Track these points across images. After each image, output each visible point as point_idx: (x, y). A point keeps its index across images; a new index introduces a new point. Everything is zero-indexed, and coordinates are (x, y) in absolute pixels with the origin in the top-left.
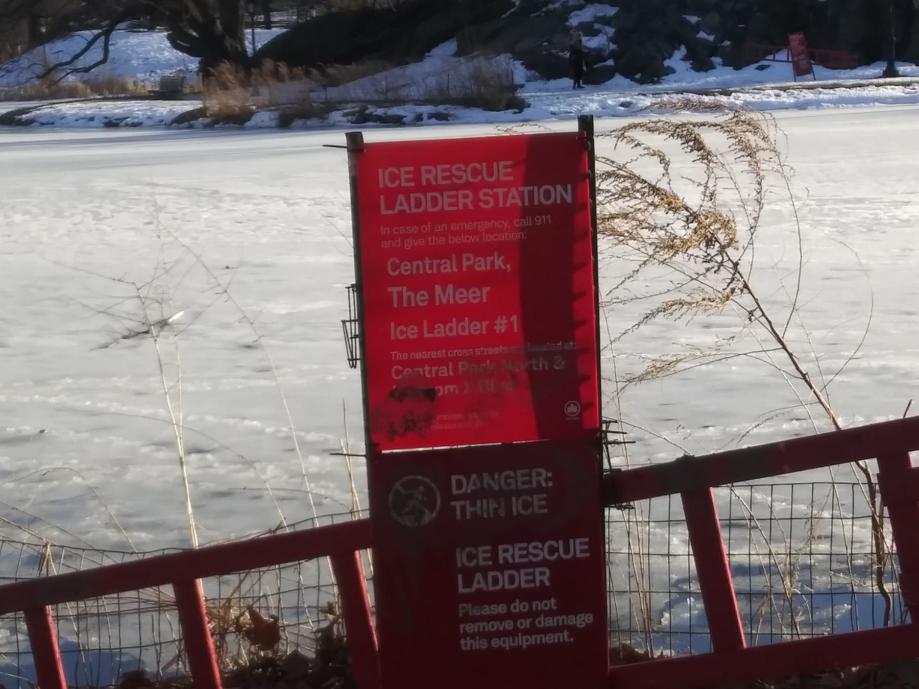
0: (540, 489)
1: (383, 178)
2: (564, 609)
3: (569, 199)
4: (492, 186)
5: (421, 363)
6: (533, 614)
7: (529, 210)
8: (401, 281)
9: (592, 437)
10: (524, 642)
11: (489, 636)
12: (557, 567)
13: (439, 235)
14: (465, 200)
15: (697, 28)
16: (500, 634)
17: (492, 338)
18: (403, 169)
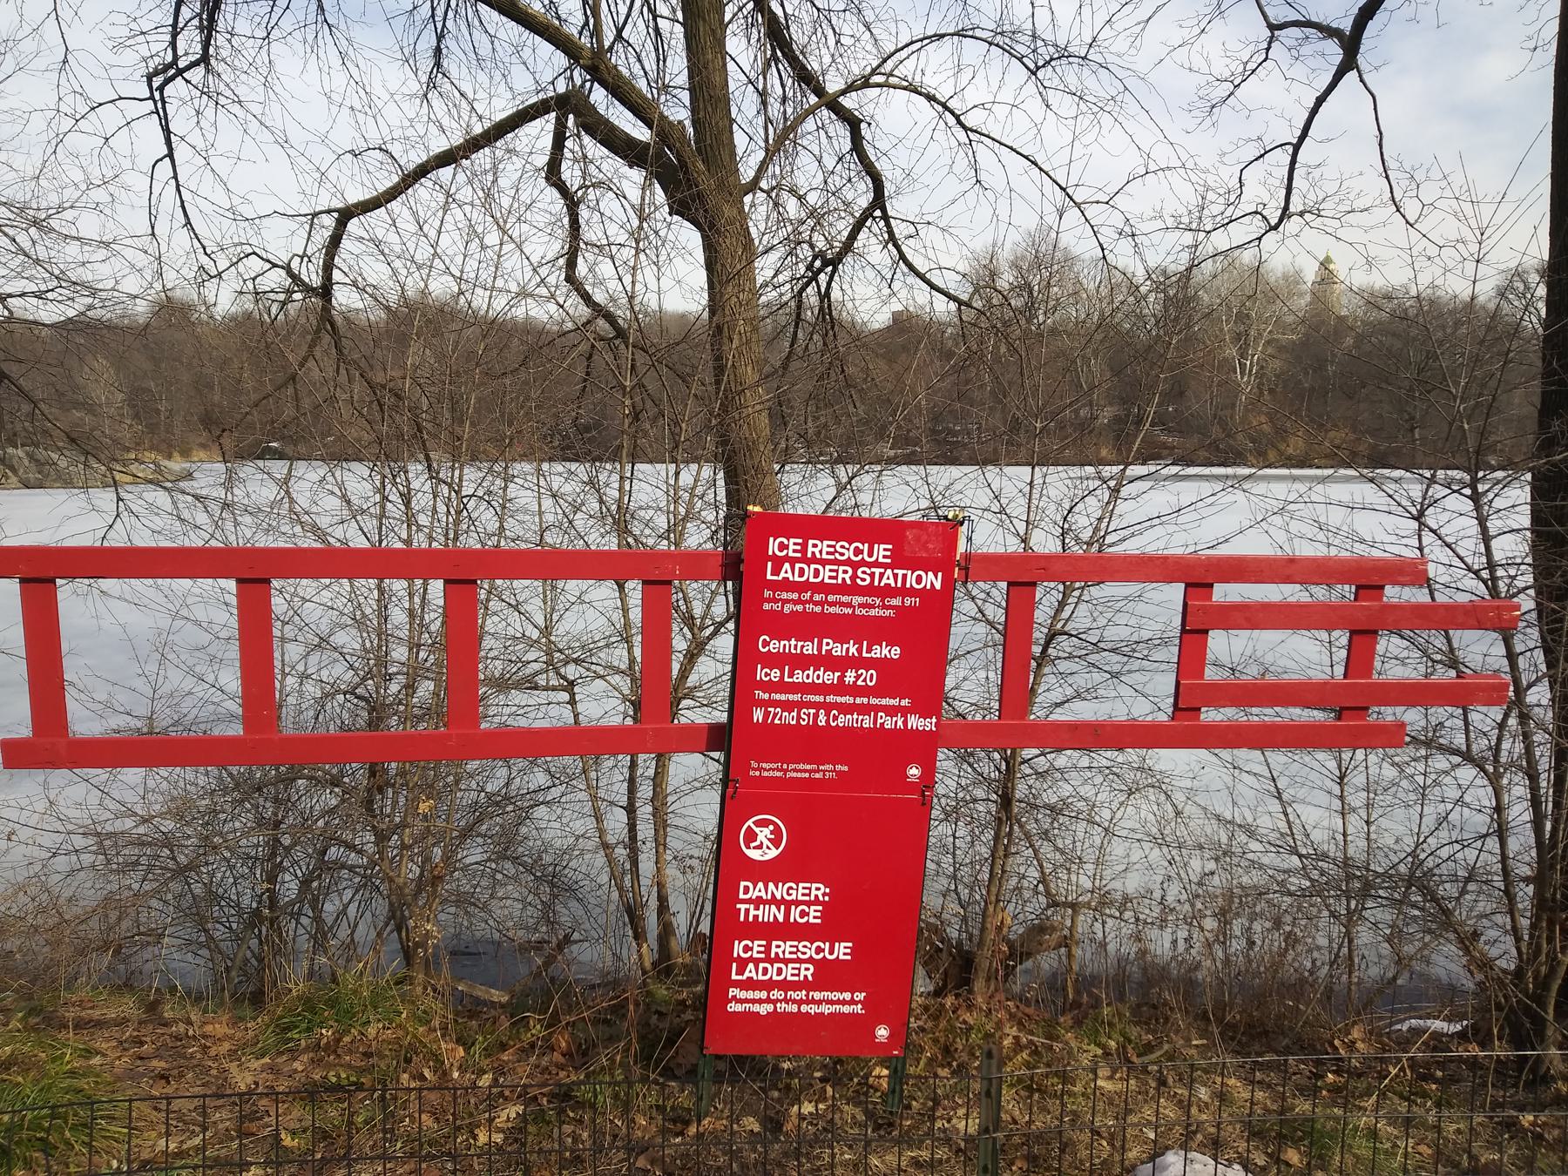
3: (938, 586)
4: (870, 565)
13: (816, 603)
14: (844, 574)
18: (792, 540)
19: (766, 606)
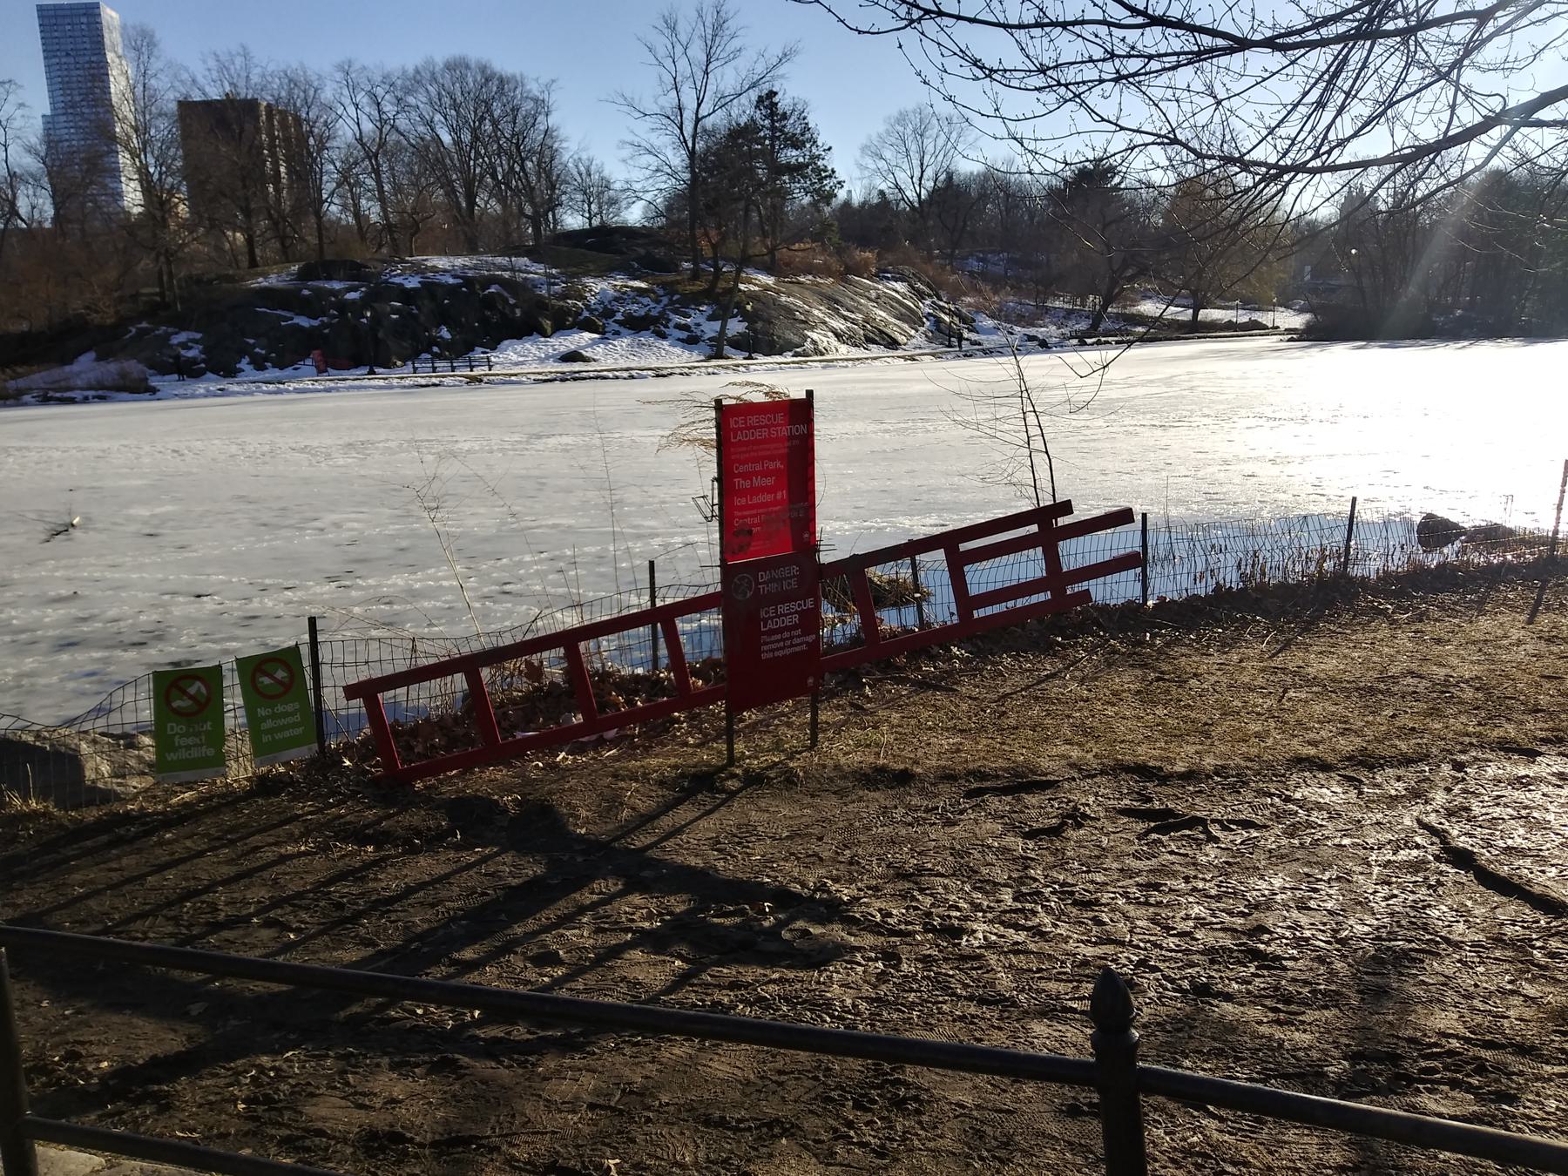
6: (791, 638)
7: (791, 438)
9: (813, 547)
10: (787, 652)
15: (254, 346)
17: (775, 503)
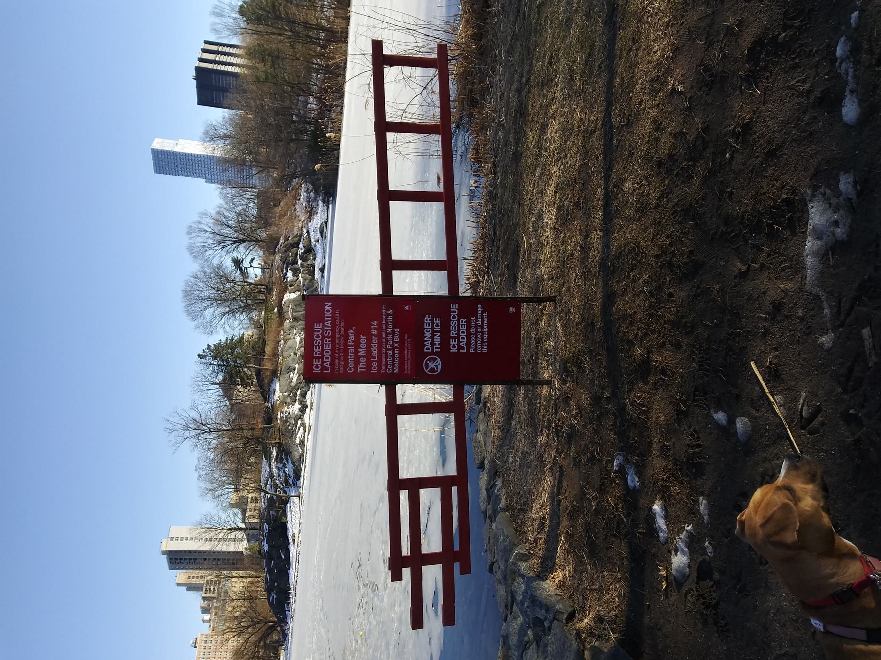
0: (432, 320)
1: (317, 370)
2: (475, 315)
4: (323, 331)
5: (386, 362)
8: (356, 368)
10: (485, 330)
11: (482, 342)
12: (460, 316)
14: (328, 341)
16: (482, 338)
19: (341, 371)
